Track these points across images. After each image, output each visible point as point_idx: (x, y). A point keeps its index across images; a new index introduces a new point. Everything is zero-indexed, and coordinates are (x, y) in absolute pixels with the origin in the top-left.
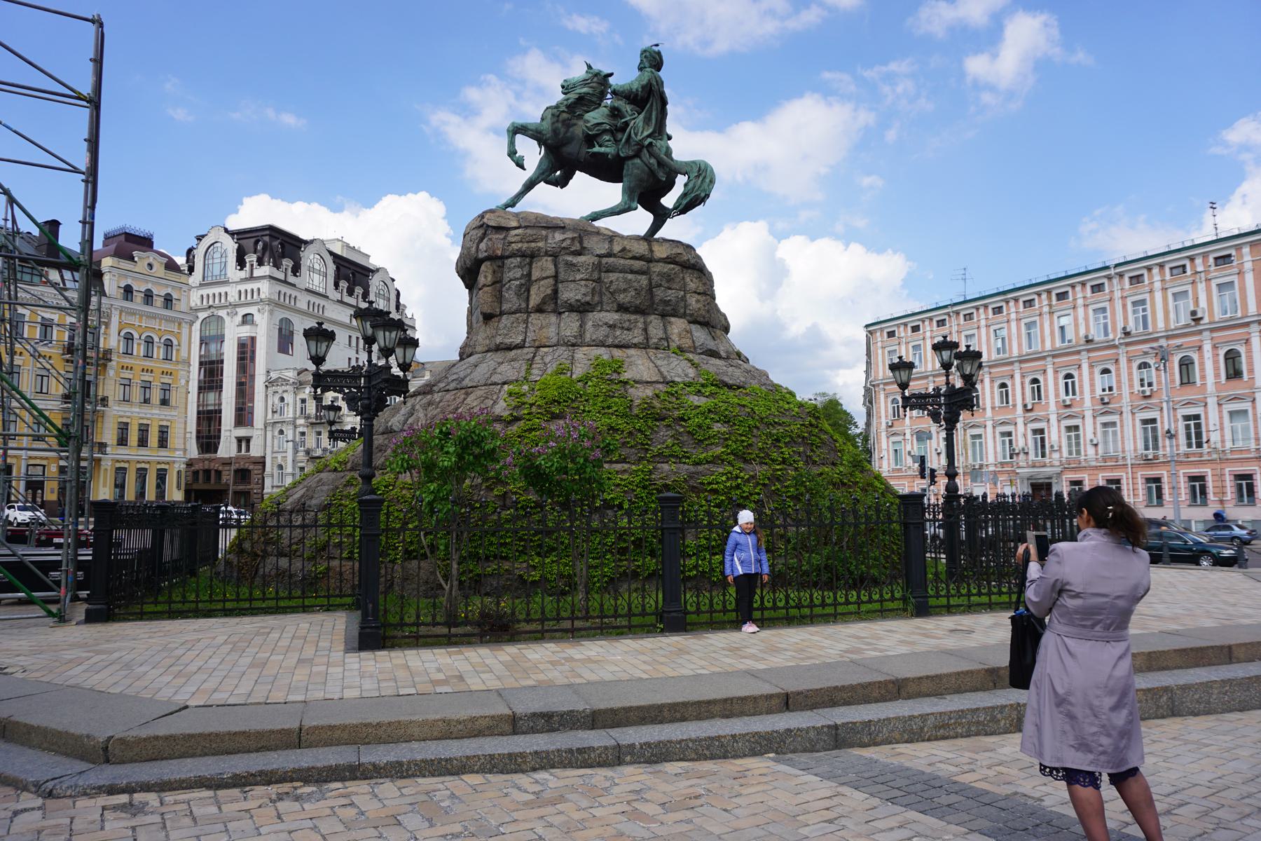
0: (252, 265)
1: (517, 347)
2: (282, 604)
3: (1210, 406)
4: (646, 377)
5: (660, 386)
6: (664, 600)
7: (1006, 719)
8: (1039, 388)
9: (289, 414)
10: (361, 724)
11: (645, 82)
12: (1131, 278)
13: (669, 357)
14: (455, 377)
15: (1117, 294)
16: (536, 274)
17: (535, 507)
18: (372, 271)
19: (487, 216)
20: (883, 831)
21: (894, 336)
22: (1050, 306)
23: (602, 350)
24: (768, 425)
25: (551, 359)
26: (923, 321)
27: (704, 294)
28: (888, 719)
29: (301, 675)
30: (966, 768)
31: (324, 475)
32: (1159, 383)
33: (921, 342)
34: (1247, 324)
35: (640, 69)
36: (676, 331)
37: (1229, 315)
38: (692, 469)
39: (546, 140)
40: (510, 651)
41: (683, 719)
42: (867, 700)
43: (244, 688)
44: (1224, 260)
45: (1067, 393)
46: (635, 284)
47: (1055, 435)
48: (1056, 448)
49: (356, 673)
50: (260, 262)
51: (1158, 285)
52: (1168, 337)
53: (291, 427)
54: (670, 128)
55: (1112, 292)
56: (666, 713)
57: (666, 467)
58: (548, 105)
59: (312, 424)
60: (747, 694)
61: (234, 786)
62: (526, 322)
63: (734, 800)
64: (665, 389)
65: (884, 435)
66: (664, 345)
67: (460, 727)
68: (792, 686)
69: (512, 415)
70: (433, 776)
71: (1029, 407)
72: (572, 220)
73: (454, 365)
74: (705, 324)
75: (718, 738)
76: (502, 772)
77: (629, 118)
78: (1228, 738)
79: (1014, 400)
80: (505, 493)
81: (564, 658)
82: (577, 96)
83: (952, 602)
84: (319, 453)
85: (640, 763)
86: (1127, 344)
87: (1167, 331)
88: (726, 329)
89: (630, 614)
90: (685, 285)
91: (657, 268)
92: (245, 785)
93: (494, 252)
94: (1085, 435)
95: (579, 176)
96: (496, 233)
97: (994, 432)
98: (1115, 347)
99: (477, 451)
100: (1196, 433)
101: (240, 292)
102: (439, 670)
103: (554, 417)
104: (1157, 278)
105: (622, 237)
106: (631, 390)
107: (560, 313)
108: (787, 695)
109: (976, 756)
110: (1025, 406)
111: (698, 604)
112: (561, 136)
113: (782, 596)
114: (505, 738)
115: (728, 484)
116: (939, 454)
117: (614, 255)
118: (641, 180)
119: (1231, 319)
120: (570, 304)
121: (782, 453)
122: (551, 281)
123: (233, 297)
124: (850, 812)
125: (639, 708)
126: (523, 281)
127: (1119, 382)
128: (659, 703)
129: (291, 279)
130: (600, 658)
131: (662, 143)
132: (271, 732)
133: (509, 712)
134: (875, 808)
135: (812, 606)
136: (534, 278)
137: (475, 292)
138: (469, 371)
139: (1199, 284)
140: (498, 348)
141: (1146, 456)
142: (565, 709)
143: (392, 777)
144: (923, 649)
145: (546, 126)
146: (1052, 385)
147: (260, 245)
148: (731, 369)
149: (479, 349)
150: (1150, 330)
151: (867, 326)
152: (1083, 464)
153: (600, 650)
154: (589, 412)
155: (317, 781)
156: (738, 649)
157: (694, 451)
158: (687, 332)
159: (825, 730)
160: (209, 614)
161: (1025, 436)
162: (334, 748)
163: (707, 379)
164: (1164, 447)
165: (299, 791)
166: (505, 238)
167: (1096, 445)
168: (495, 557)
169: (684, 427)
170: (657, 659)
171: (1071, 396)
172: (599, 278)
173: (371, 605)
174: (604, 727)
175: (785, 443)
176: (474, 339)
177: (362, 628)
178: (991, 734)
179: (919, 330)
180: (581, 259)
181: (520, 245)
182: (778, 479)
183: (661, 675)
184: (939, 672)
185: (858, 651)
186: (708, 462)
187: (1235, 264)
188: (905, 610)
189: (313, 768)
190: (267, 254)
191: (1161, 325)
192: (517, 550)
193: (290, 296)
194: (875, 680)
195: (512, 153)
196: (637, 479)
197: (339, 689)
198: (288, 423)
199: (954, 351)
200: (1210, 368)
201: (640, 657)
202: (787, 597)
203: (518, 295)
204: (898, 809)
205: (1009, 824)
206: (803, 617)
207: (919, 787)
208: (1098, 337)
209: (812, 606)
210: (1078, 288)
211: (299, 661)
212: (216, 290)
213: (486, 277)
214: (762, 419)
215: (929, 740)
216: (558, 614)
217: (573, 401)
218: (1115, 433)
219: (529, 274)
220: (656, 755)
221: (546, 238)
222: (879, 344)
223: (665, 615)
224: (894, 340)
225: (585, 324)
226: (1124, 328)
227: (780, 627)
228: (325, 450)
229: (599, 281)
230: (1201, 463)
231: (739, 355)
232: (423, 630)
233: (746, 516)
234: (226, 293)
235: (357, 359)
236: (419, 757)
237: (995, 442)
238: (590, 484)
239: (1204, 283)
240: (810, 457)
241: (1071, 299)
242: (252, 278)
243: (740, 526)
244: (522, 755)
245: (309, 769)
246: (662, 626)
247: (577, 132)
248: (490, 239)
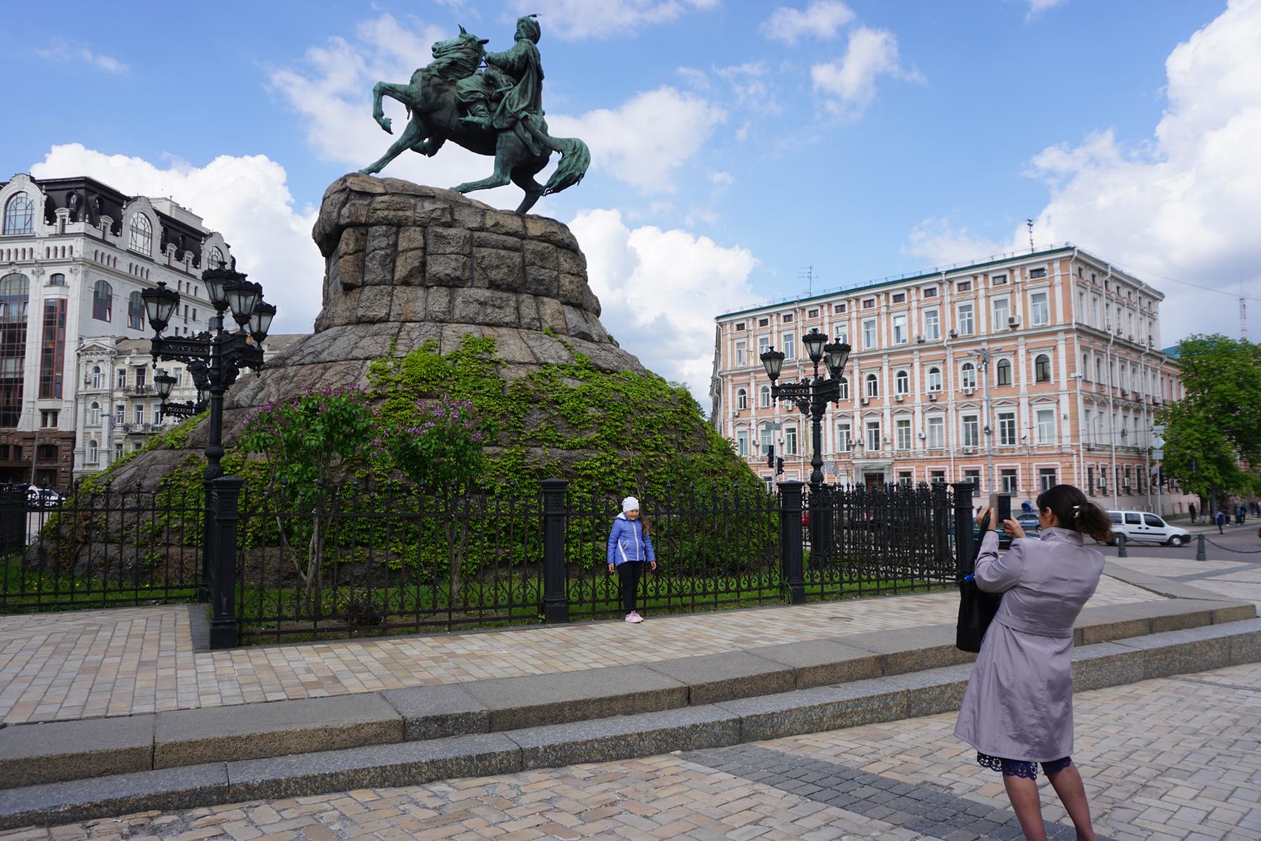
0: (64, 221)
1: (381, 321)
2: (110, 597)
3: (1022, 406)
4: (519, 358)
5: (534, 367)
6: (545, 590)
7: (897, 705)
8: (875, 383)
9: (105, 385)
10: (228, 738)
11: (521, 53)
12: (959, 285)
13: (542, 338)
14: (311, 350)
15: (947, 299)
16: (403, 245)
17: (400, 491)
18: (206, 236)
19: (350, 180)
20: (811, 831)
21: (743, 328)
22: (888, 307)
23: (472, 328)
24: (642, 411)
25: (418, 335)
26: (771, 316)
27: (577, 275)
28: (790, 710)
29: (145, 680)
30: (871, 757)
31: (158, 453)
32: (980, 383)
33: (768, 336)
34: (1055, 333)
35: (517, 39)
36: (549, 312)
37: (1040, 324)
38: (566, 453)
39: (416, 104)
40: (383, 648)
41: (584, 718)
42: (766, 691)
43: (76, 699)
44: (1038, 273)
45: (900, 390)
46: (508, 261)
47: (888, 429)
48: (888, 441)
49: (213, 677)
50: (74, 218)
51: (982, 293)
52: (989, 341)
53: (107, 400)
54: (544, 107)
55: (942, 297)
56: (567, 712)
57: (539, 451)
58: (419, 67)
59: (132, 397)
60: (649, 689)
61: (74, 820)
62: (391, 294)
63: (652, 805)
64: (539, 371)
65: (730, 425)
66: (536, 325)
67: (344, 736)
68: (694, 679)
69: (375, 392)
70: (316, 794)
71: (866, 402)
72: (442, 190)
73: (309, 337)
74: (578, 306)
75: (624, 737)
76: (394, 786)
77: (503, 89)
78: (1092, 716)
79: (853, 395)
80: (368, 475)
81: (446, 654)
82: (450, 61)
83: (825, 590)
84: (139, 429)
85: (544, 767)
86: (954, 346)
87: (988, 335)
88: (598, 313)
89: (511, 605)
90: (559, 265)
91: (531, 246)
92: (87, 818)
93: (357, 218)
94: (914, 430)
95: (449, 145)
96: (360, 199)
97: (833, 425)
98: (943, 348)
99: (346, 428)
100: (1009, 432)
101: (48, 249)
102: (309, 671)
103: (423, 396)
104: (982, 286)
105: (495, 211)
106: (503, 371)
107: (428, 287)
108: (689, 689)
109: (877, 745)
110: (862, 400)
111: (581, 593)
112: (432, 101)
113: (689, 584)
114: (395, 746)
115: (602, 470)
116: (781, 444)
117: (487, 230)
118: (515, 154)
119: (1043, 327)
120: (439, 278)
121: (655, 439)
122: (419, 253)
123: (40, 254)
124: (773, 812)
125: (539, 708)
126: (388, 251)
127: (946, 380)
128: (560, 701)
129: (110, 238)
130: (484, 653)
131: (537, 117)
132: (118, 752)
133: (399, 718)
134: (796, 805)
135: (693, 594)
136: (400, 249)
137: (333, 260)
138: (327, 344)
140: (359, 321)
141: (967, 450)
142: (460, 712)
143: (268, 798)
144: (810, 637)
145: (416, 89)
146: (887, 381)
147: (74, 200)
148: (603, 353)
149: (337, 321)
150: (974, 334)
151: (718, 318)
152: (912, 457)
153: (482, 644)
154: (459, 391)
155: (178, 808)
156: (626, 640)
157: (569, 436)
158: (560, 313)
159: (730, 724)
160: (20, 610)
161: (861, 429)
162: (195, 767)
163: (581, 362)
164: (982, 442)
165: (157, 822)
166: (369, 205)
167: (924, 439)
168: (357, 543)
169: (558, 410)
170: (546, 652)
171: (903, 393)
172: (471, 253)
173: (225, 599)
174: (502, 730)
175: (658, 430)
176: (333, 310)
177: (214, 625)
178: (884, 721)
179: (767, 324)
180: (452, 231)
181: (386, 213)
182: (651, 466)
183: (554, 671)
184: (833, 661)
185: (749, 641)
186: (582, 447)
187: (1047, 277)
188: (782, 598)
189: (173, 793)
190: (82, 209)
191: (983, 330)
192: (380, 537)
193: (109, 257)
194: (773, 671)
195: (378, 115)
196: (509, 463)
197: (194, 696)
198: (104, 396)
199: (823, 344)
200: (1023, 372)
201: (527, 650)
202: (670, 585)
203: (383, 266)
204: (821, 805)
205: (928, 815)
206: (685, 606)
207: (833, 780)
208: (929, 338)
209: (716, 592)
210: (913, 291)
211: (141, 664)
212: (20, 246)
213: (347, 245)
214: (636, 404)
215: (827, 730)
216: (435, 606)
217: (442, 380)
218: (940, 428)
219: (396, 245)
220: (560, 758)
221: (415, 207)
222: (729, 336)
223: (547, 605)
224: (743, 333)
225: (455, 300)
226: (952, 331)
227: (662, 616)
228: (147, 426)
229: (470, 255)
230: (1013, 457)
231: (611, 339)
232: (285, 625)
233: (631, 504)
234: (32, 250)
235: (186, 329)
236: (300, 774)
237: (834, 434)
238: (466, 464)
240: (682, 444)
241: (906, 301)
242: (63, 234)
243: (625, 514)
244: (417, 765)
245: (168, 795)
246: (544, 617)
248: (354, 205)
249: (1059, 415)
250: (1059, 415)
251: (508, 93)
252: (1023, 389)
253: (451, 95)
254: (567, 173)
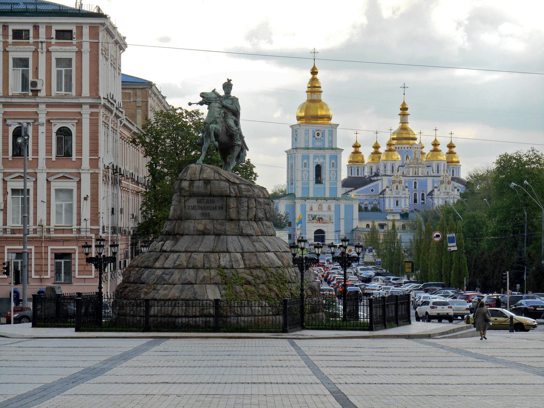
16: (251, 206)
34: (80, 105)
37: (63, 92)
96: (233, 185)
122: (255, 209)
139: (40, 53)
187: (74, 41)
213: (234, 204)
239: (45, 53)
249: (79, 195)
250: (79, 195)
252: (42, 163)
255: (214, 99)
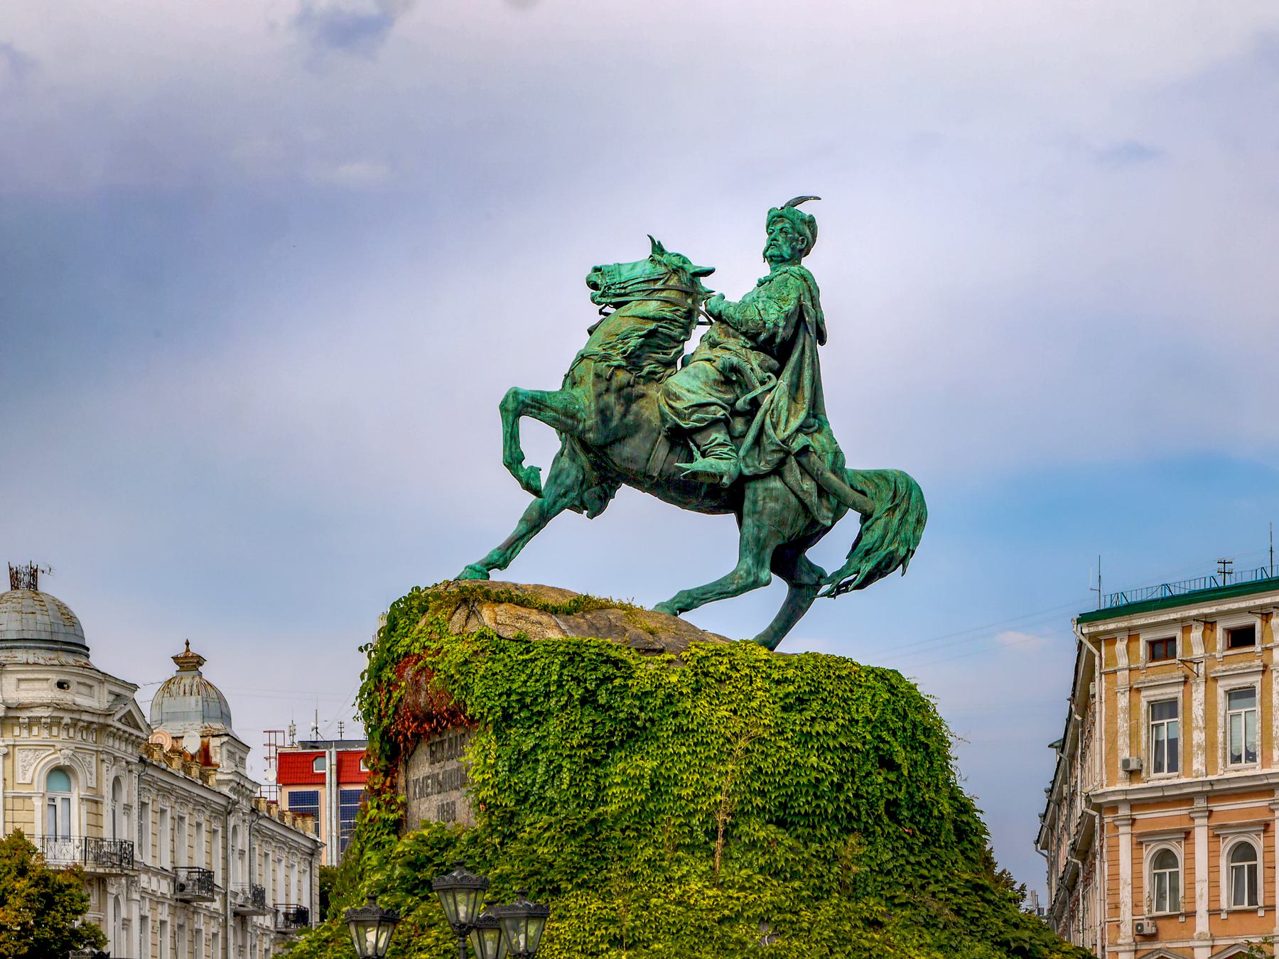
11: (790, 307)
39: (584, 431)
77: (760, 390)
112: (614, 423)
151: (1085, 619)
195: (514, 460)
247: (646, 414)
251: (768, 397)
253: (652, 405)
254: (882, 553)
255: (644, 286)
